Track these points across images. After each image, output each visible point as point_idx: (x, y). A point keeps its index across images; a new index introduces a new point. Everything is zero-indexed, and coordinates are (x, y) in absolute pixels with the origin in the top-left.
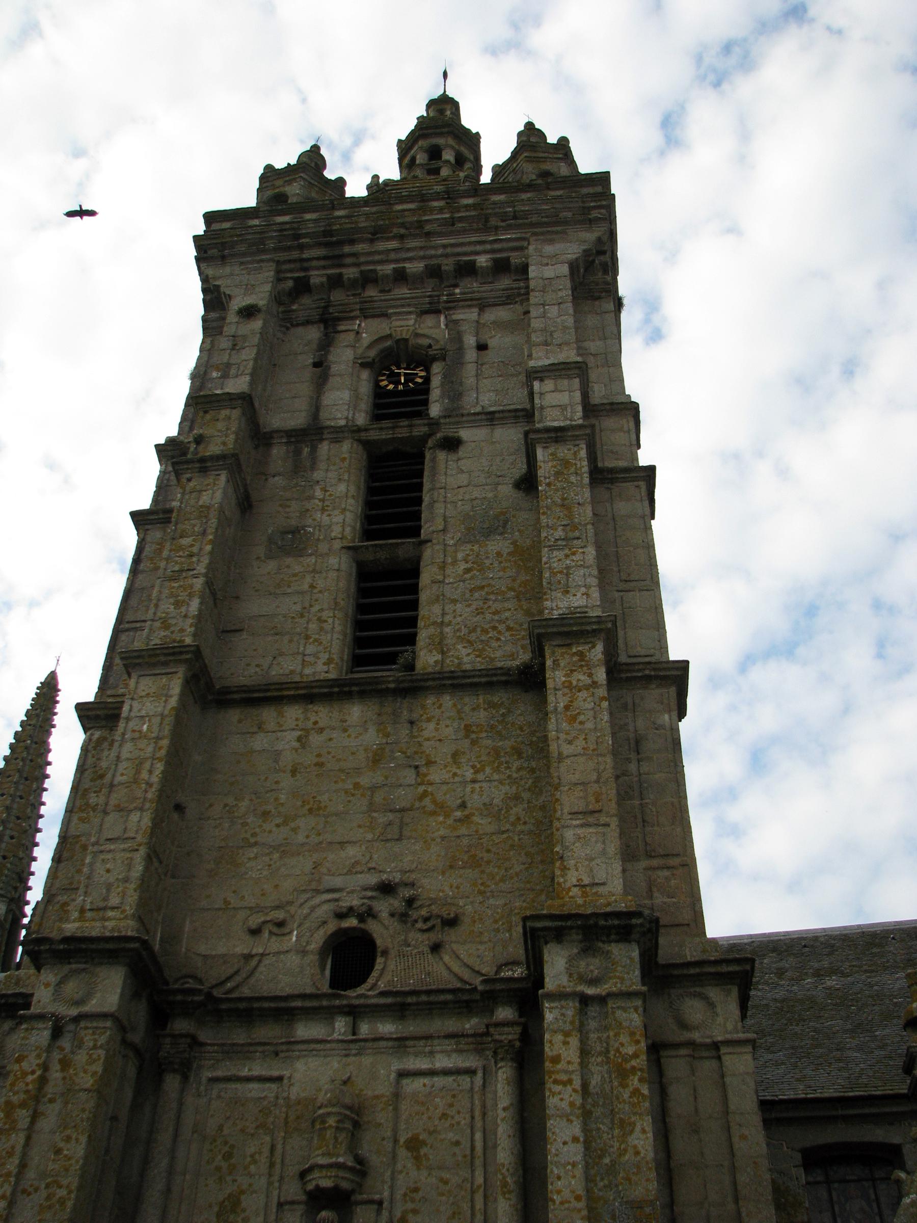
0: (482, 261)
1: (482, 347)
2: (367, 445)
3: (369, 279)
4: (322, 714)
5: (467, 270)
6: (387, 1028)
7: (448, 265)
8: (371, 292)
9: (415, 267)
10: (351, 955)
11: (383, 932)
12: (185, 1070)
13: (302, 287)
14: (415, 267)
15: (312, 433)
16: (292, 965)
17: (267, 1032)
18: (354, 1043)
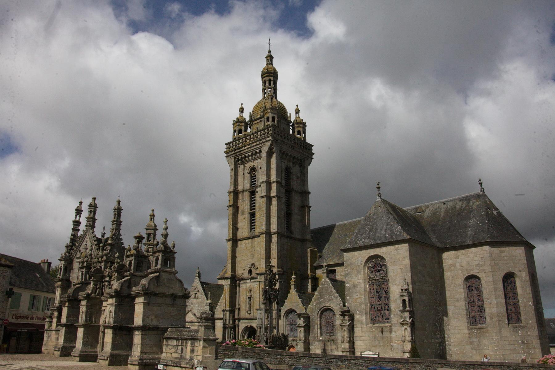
0: (258, 151)
1: (261, 168)
2: (250, 192)
3: (245, 157)
4: (247, 241)
5: (256, 152)
6: (253, 280)
7: (254, 152)
8: (247, 159)
9: (250, 154)
10: (250, 272)
11: (252, 269)
12: (239, 286)
13: (238, 160)
14: (250, 154)
15: (243, 191)
16: (246, 275)
17: (245, 281)
18: (250, 282)
